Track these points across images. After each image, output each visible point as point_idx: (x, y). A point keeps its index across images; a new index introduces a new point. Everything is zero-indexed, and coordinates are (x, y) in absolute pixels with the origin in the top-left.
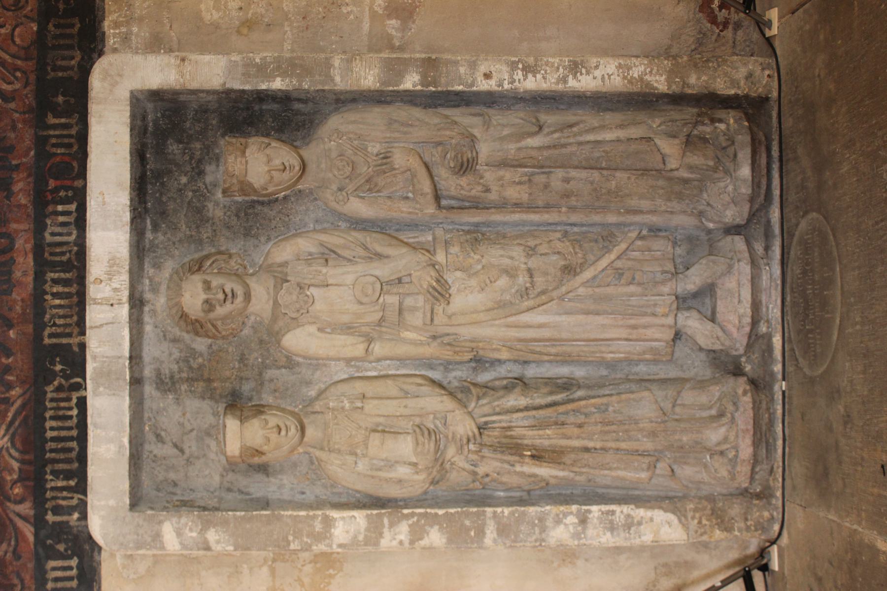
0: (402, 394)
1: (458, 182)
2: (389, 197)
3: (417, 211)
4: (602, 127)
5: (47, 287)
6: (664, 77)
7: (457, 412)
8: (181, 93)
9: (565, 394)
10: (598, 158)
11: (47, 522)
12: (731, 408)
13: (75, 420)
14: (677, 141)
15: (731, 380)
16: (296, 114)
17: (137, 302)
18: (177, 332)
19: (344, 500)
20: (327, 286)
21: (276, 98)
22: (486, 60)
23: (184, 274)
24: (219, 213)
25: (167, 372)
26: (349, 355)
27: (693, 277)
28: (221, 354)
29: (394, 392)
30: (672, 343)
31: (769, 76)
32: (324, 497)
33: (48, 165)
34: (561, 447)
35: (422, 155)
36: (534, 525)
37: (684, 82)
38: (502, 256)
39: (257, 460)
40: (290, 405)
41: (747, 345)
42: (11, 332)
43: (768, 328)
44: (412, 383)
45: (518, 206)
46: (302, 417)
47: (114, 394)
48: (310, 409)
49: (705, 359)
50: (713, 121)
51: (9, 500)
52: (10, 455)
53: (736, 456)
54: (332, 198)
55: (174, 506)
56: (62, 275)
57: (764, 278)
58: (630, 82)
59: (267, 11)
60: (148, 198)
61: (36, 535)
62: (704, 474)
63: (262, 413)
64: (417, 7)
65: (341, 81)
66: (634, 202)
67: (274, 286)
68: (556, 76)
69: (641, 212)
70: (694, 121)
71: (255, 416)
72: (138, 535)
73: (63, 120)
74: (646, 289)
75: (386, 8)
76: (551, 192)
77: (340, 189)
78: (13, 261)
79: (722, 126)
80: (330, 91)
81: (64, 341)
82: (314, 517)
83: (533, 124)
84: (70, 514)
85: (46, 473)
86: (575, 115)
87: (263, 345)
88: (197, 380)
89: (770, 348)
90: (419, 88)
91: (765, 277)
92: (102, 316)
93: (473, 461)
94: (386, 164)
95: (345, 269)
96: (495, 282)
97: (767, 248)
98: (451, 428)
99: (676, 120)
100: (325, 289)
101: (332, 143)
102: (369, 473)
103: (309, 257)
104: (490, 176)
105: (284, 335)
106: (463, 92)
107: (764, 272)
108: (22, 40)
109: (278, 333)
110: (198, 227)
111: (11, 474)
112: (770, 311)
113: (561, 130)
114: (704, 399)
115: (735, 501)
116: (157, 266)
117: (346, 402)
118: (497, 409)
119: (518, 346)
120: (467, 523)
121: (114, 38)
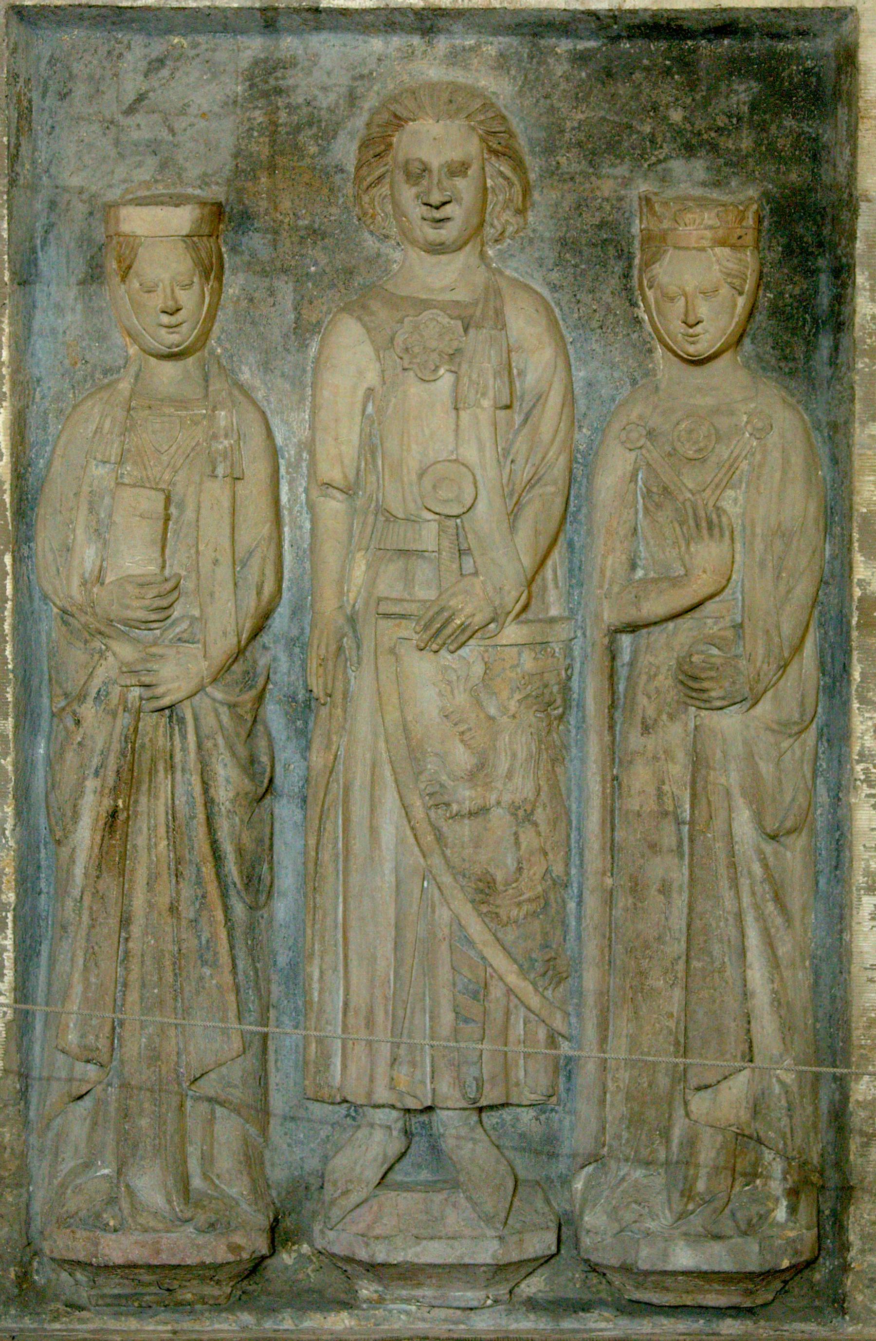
0: (241, 554)
1: (664, 670)
3: (606, 586)
4: (774, 962)
7: (204, 664)
8: (850, 110)
9: (237, 880)
10: (710, 954)
15: (263, 1221)
16: (808, 343)
17: (428, 23)
18: (370, 102)
20: (456, 409)
21: (840, 304)
23: (482, 122)
24: (607, 188)
25: (291, 82)
28: (326, 191)
30: (338, 1099)
32: (38, 396)
34: (133, 871)
35: (717, 599)
38: (514, 756)
40: (223, 331)
41: (333, 1255)
43: (368, 1301)
46: (198, 354)
48: (214, 369)
50: (793, 1193)
54: (634, 416)
57: (469, 1294)
60: (640, 42)
62: (72, 1164)
67: (458, 302)
69: (603, 1040)
76: (643, 856)
77: (651, 434)
79: (781, 1214)
80: (852, 413)
83: (782, 823)
87: (342, 276)
88: (273, 143)
90: (857, 592)
91: (471, 1296)
93: (108, 694)
94: (697, 525)
95: (489, 445)
96: (462, 741)
97: (532, 1305)
99: (791, 1117)
100: (449, 405)
102: (86, 489)
103: (515, 371)
105: (359, 319)
106: (849, 682)
107: (481, 1294)
109: (364, 307)
110: (580, 144)
112: (404, 1306)
113: (769, 876)
115: (17, 1227)
116: (502, 63)
117: (226, 443)
118: (209, 744)
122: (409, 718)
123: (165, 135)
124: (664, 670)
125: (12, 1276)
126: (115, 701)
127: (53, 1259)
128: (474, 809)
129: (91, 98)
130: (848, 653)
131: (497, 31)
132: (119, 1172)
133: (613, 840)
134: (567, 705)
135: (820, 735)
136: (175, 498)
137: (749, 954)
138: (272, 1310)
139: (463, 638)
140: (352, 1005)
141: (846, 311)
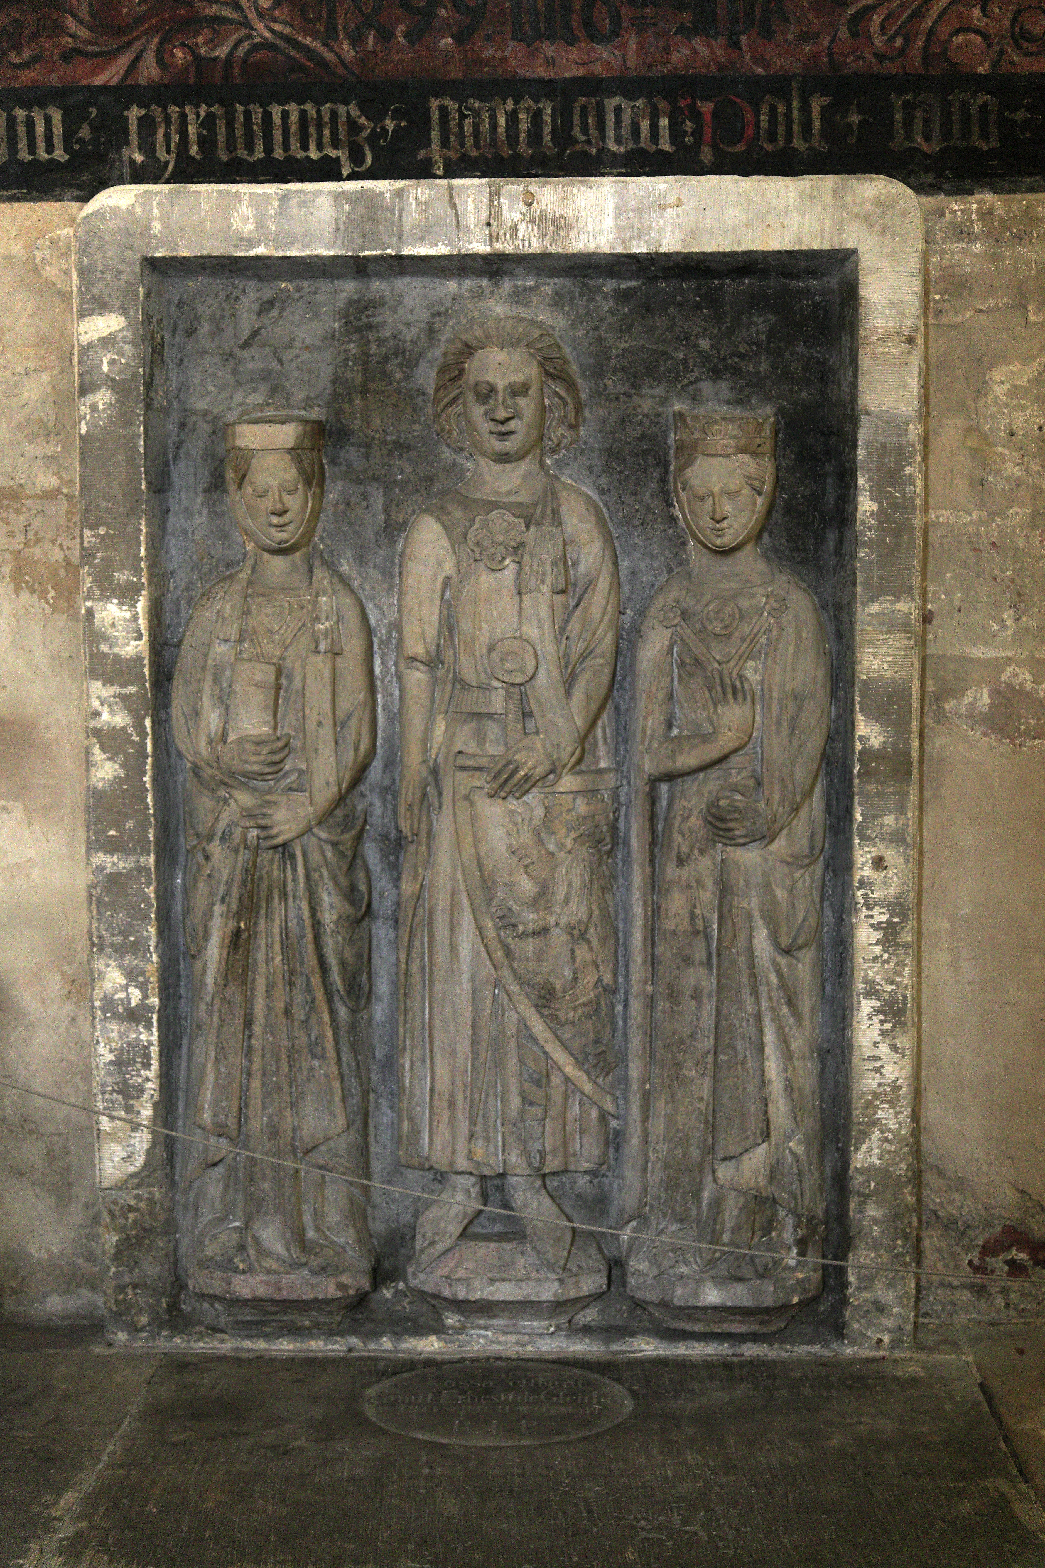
0: (341, 716)
1: (696, 812)
2: (671, 696)
4: (787, 1056)
5: (527, 102)
6: (877, 1162)
7: (311, 809)
8: (852, 337)
9: (341, 988)
11: (127, 108)
12: (315, 1262)
13: (300, 155)
14: (762, 1181)
15: (365, 1264)
17: (495, 267)
19: (167, 619)
20: (520, 593)
22: (907, 861)
23: (540, 349)
24: (647, 405)
25: (379, 319)
26: (407, 629)
27: (535, 1204)
28: (409, 410)
29: (345, 703)
31: (880, 1341)
32: (172, 585)
33: (738, 100)
34: (254, 980)
36: (125, 934)
37: (868, 1196)
38: (570, 885)
39: (230, 475)
40: (324, 530)
42: (449, 40)
43: (452, 1327)
44: (360, 734)
45: (655, 913)
47: (338, 229)
48: (317, 562)
49: (402, 1221)
51: (161, 43)
52: (239, 42)
53: (236, 1270)
55: (152, 333)
56: (547, 129)
57: (536, 1324)
58: (869, 1104)
59: (1008, 479)
61: (104, 89)
62: (209, 1217)
63: (308, 483)
64: (1012, 739)
65: (870, 614)
66: (661, 1106)
68: (878, 978)
69: (645, 1119)
70: (800, 1210)
71: (302, 471)
72: (103, 272)
73: (817, 124)
74: (514, 1125)
75: (1010, 686)
77: (684, 615)
78: (572, 41)
80: (854, 594)
81: (435, 134)
82: (137, 571)
83: (795, 939)
84: (140, 149)
85: (210, 105)
86: (813, 1009)
88: (365, 370)
89: (420, 1330)
90: (858, 746)
91: (537, 1324)
92: (471, 207)
93: (231, 834)
95: (547, 623)
96: (526, 873)
97: (587, 1330)
98: (284, 799)
99: (801, 1181)
100: (514, 590)
101: (764, 600)
102: (210, 662)
104: (704, 865)
105: (438, 519)
107: (546, 1323)
108: (960, 46)
109: (442, 508)
110: (623, 369)
111: (206, 43)
112: (483, 1332)
113: (783, 985)
114: (333, 1218)
115: (166, 1266)
116: (557, 301)
117: (327, 624)
118: (315, 876)
119: (421, 910)
120: (130, 824)
121: (962, 211)
122: (482, 854)
123: (275, 365)
124: (696, 812)
125: (164, 1305)
126: (237, 841)
127: (196, 1294)
128: (537, 929)
129: (213, 335)
130: (851, 798)
131: (554, 272)
132: (247, 1226)
133: (653, 954)
134: (614, 844)
135: (827, 867)
136: (285, 671)
137: (767, 1050)
138: (375, 1335)
139: (527, 787)
140: (436, 1090)
141: (850, 508)
